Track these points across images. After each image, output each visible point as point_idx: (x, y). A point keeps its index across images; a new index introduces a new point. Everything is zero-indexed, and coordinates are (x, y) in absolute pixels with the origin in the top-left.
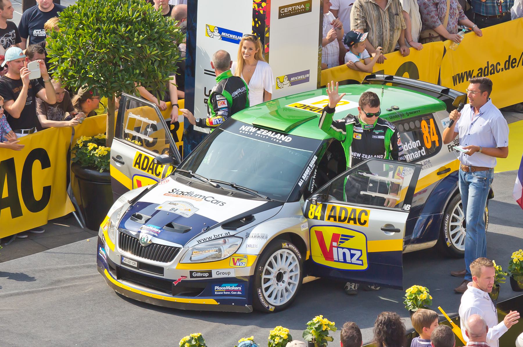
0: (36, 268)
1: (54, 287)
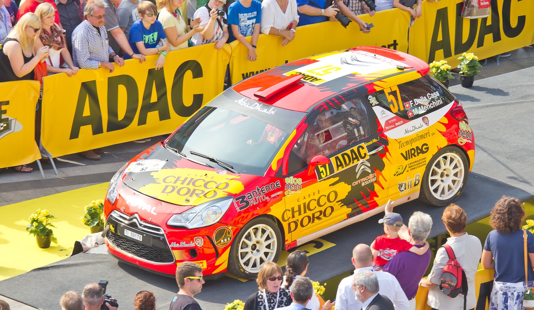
0: (510, 84)
1: (524, 100)
